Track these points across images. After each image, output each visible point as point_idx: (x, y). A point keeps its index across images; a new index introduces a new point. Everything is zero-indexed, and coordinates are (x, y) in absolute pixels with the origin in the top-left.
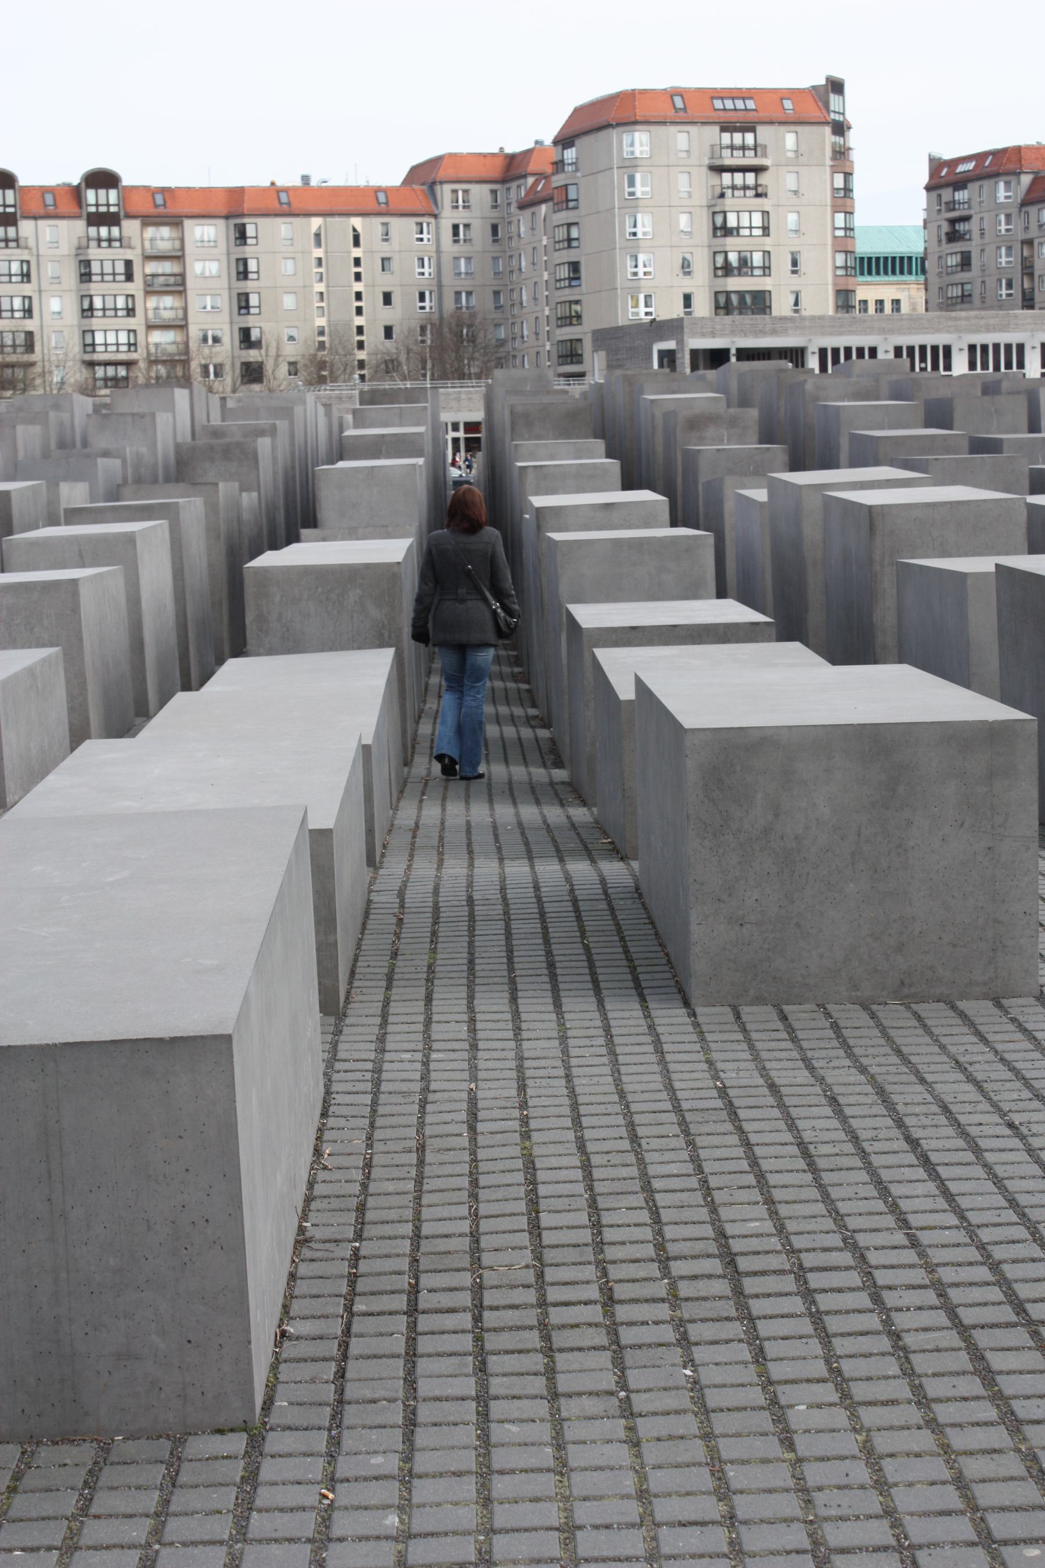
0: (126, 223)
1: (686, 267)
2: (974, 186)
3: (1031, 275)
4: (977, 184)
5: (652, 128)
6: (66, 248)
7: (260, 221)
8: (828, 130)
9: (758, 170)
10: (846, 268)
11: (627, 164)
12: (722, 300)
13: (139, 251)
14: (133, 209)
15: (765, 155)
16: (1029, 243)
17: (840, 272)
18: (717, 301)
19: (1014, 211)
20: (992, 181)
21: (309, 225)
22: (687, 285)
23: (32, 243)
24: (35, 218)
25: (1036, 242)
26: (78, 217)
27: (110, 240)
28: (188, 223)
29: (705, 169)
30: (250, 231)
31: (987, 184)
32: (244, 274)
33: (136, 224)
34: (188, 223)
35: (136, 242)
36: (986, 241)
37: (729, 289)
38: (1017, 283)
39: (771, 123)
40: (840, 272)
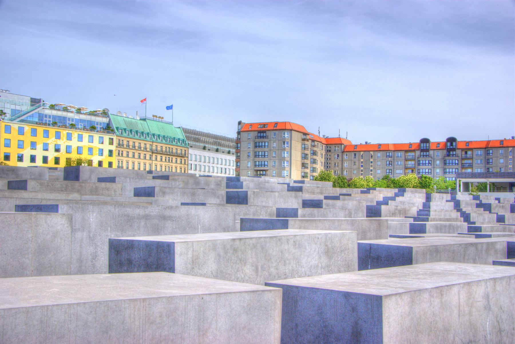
0: (457, 150)
6: (441, 157)
7: (493, 149)
13: (460, 157)
14: (458, 147)
21: (508, 150)
23: (432, 156)
24: (434, 150)
26: (445, 149)
27: (453, 155)
28: (474, 150)
30: (491, 152)
32: (488, 163)
33: (460, 150)
34: (474, 150)
35: (460, 155)
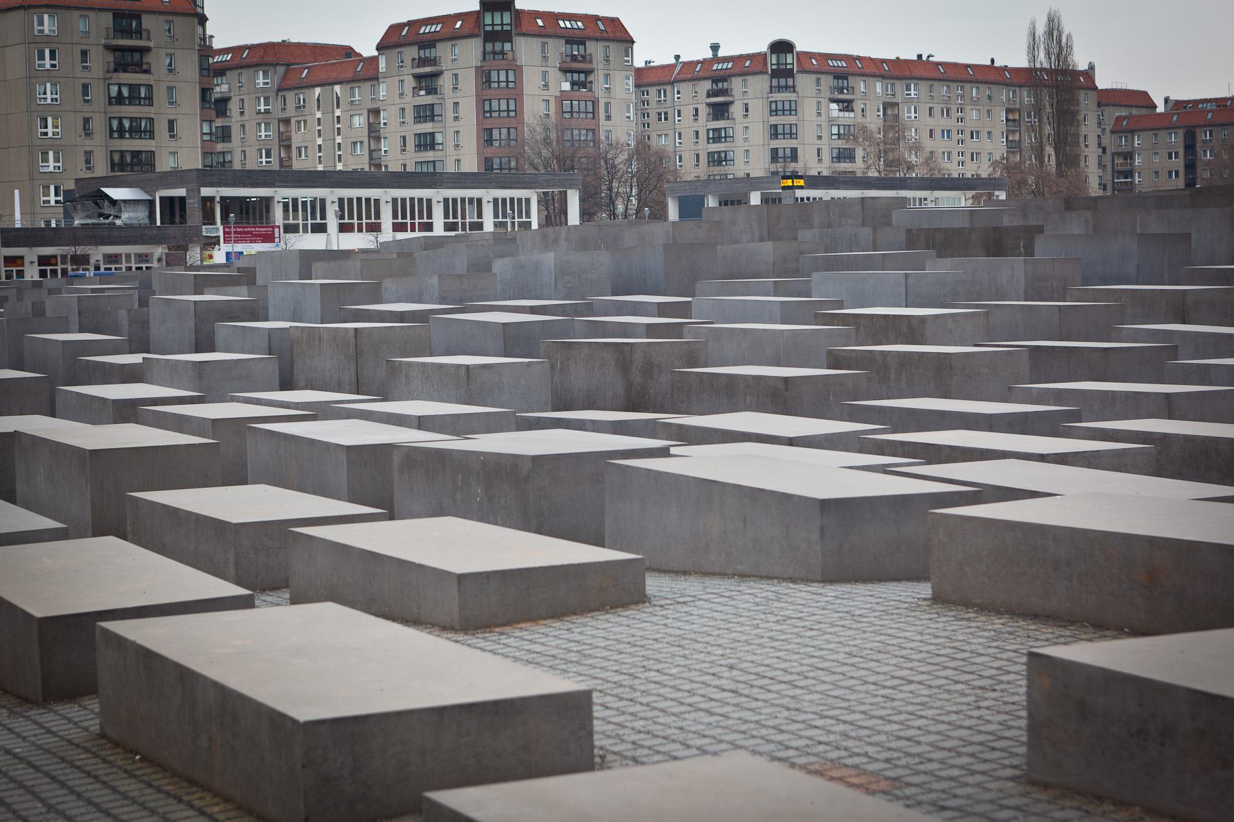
1: (88, 133)
2: (232, 75)
3: (288, 147)
4: (236, 72)
5: (59, 11)
8: (196, 20)
9: (145, 50)
10: (210, 134)
11: (38, 40)
12: (116, 157)
15: (149, 39)
16: (287, 121)
17: (206, 138)
18: (112, 160)
19: (272, 95)
20: (251, 71)
22: (88, 144)
25: (293, 121)
29: (101, 48)
31: (246, 73)
36: (246, 117)
37: (124, 148)
38: (274, 153)
39: (153, 12)
40: (206, 138)
